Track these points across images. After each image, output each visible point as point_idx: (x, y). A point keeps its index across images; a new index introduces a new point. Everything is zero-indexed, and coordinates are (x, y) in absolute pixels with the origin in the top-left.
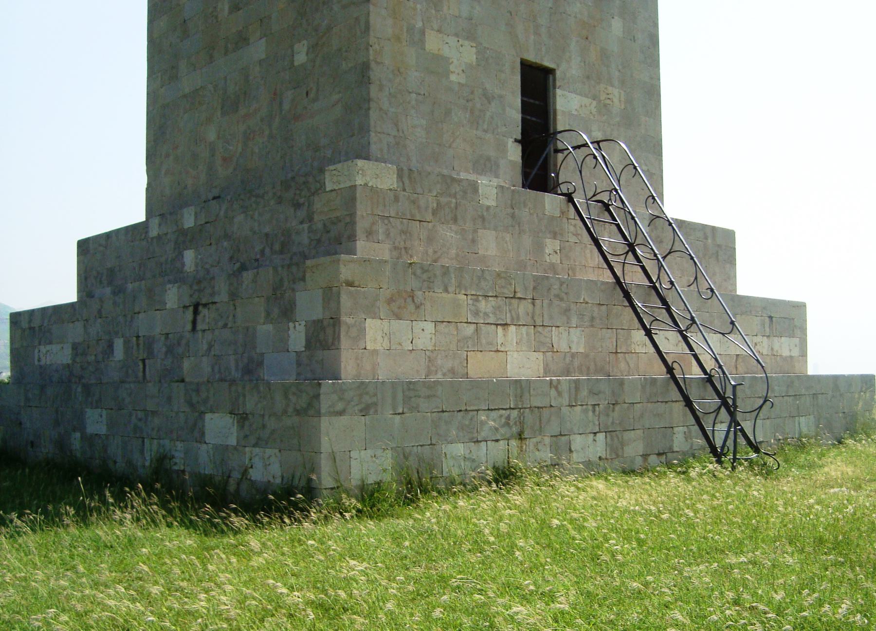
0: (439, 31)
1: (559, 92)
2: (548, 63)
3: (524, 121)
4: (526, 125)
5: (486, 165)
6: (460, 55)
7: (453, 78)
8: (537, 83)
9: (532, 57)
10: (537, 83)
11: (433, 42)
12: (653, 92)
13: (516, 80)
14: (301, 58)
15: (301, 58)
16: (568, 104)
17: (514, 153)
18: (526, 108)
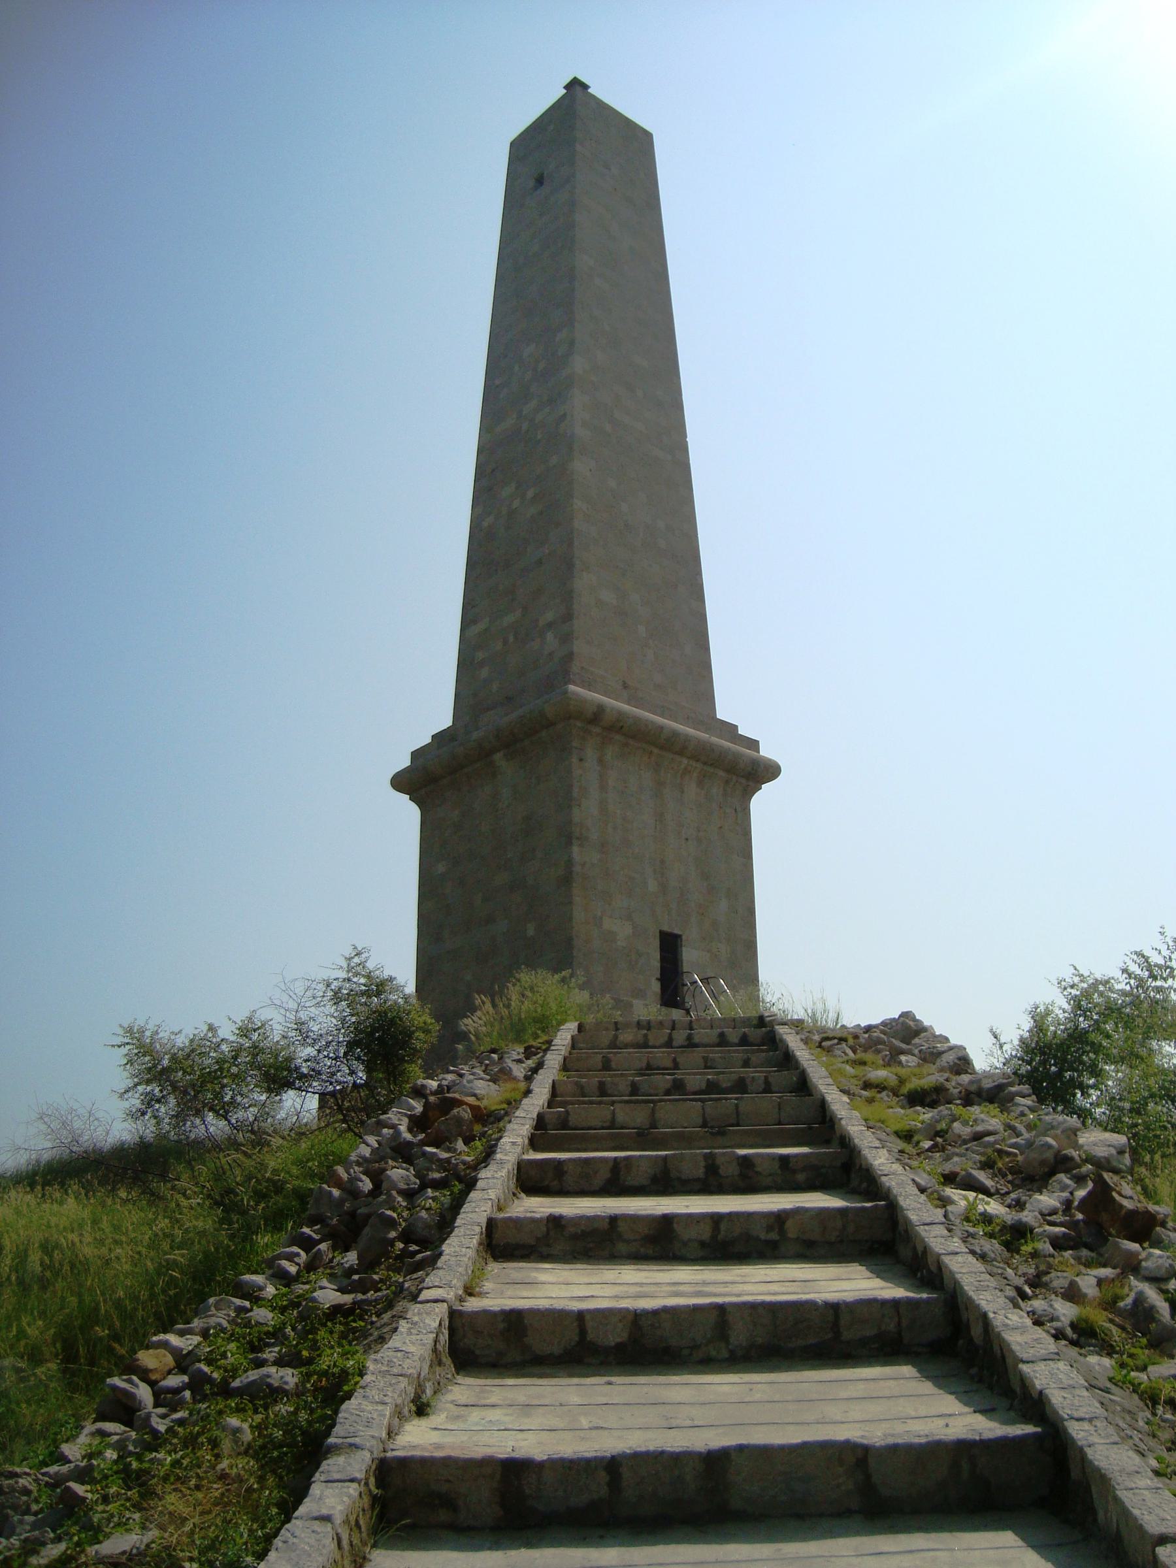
0: (611, 917)
1: (684, 949)
2: (676, 931)
3: (662, 967)
4: (663, 970)
5: (639, 993)
6: (622, 931)
7: (619, 943)
8: (670, 945)
9: (666, 928)
10: (670, 945)
11: (607, 924)
12: (750, 946)
13: (657, 943)
14: (531, 932)
15: (531, 932)
16: (690, 955)
17: (656, 987)
18: (663, 959)
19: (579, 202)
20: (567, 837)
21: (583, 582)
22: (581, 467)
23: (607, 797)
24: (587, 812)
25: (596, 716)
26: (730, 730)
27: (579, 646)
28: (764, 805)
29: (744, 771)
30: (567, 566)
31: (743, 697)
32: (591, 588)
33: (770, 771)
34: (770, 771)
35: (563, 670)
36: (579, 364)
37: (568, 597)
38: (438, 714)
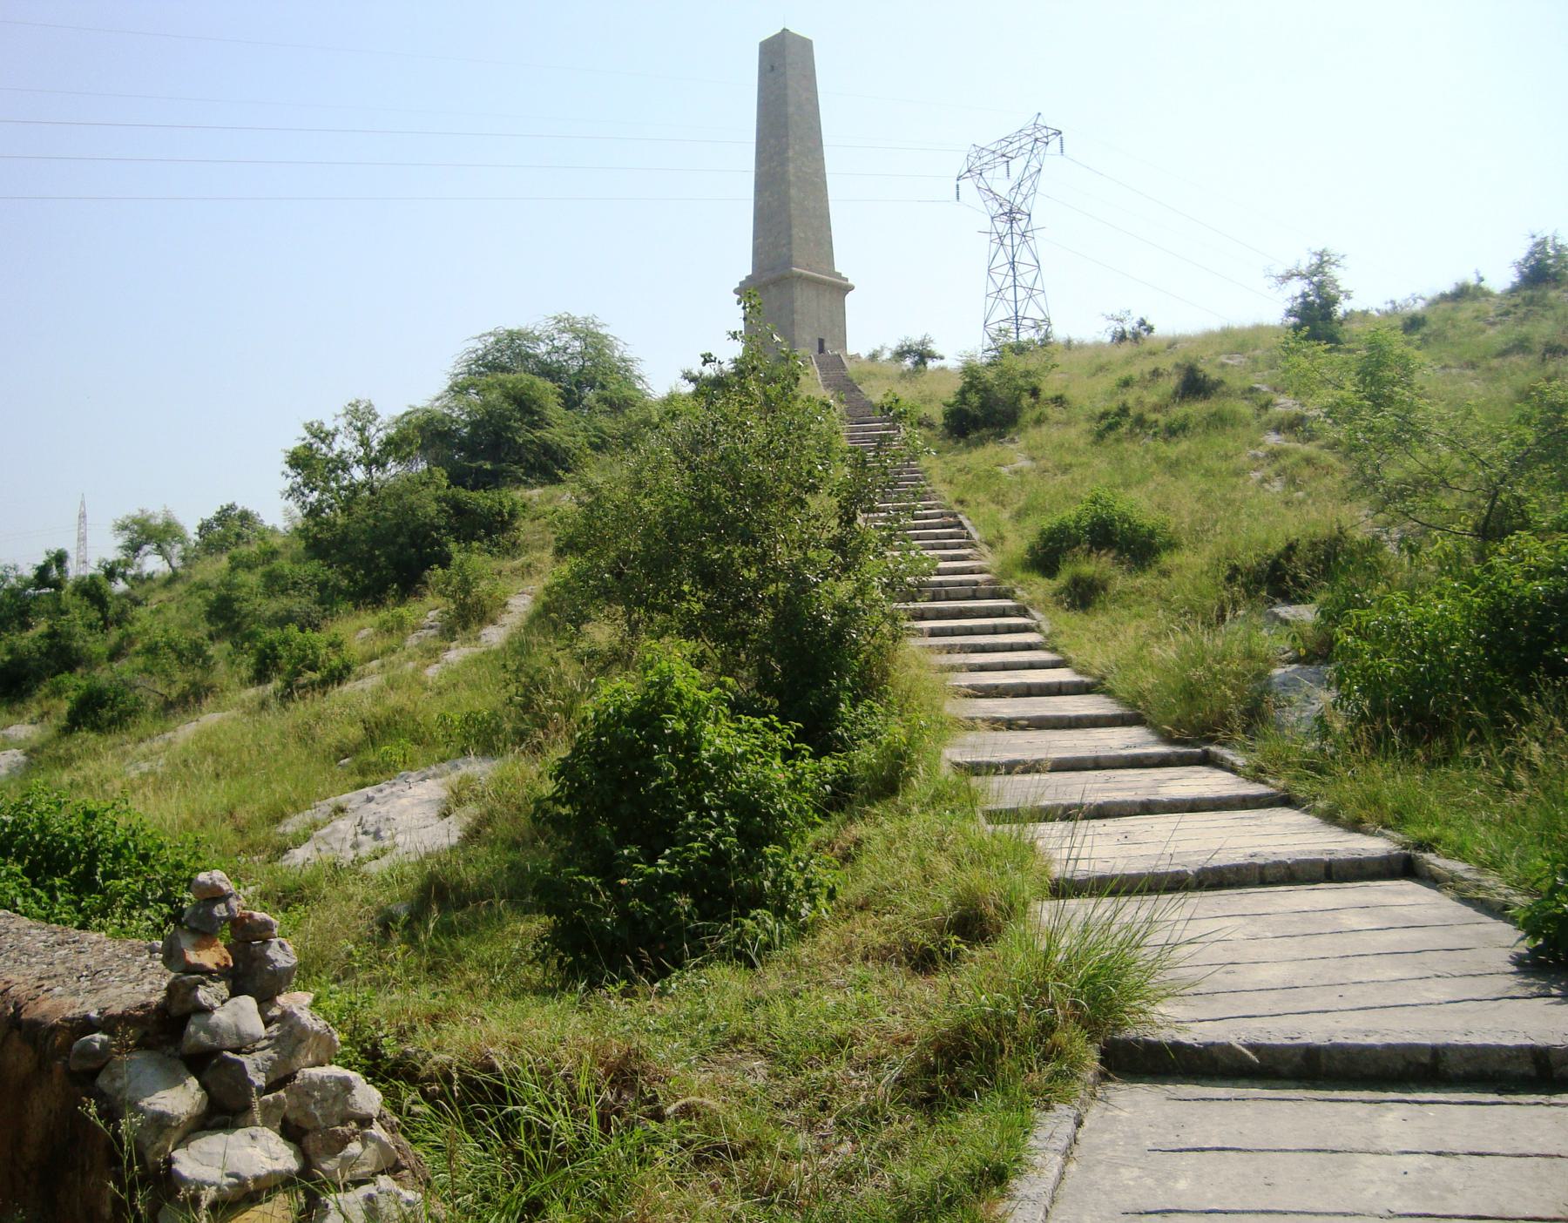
6: (808, 338)
10: (821, 342)
16: (826, 345)
19: (784, 71)
20: (793, 312)
21: (795, 231)
22: (793, 192)
23: (803, 299)
24: (798, 304)
25: (800, 276)
26: (839, 275)
27: (795, 253)
28: (849, 298)
29: (844, 289)
30: (789, 228)
31: (844, 264)
32: (797, 232)
33: (851, 288)
34: (851, 288)
35: (789, 263)
36: (791, 153)
37: (790, 236)
38: (748, 270)
